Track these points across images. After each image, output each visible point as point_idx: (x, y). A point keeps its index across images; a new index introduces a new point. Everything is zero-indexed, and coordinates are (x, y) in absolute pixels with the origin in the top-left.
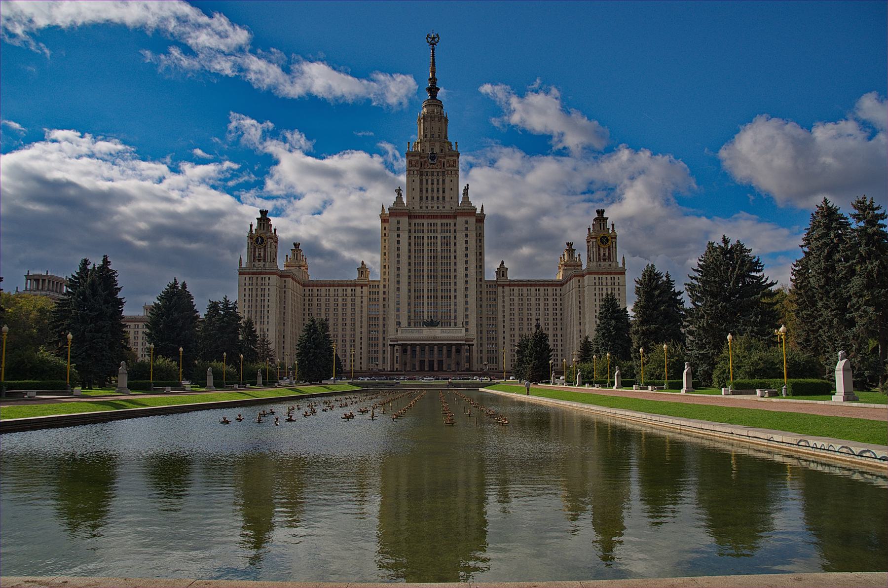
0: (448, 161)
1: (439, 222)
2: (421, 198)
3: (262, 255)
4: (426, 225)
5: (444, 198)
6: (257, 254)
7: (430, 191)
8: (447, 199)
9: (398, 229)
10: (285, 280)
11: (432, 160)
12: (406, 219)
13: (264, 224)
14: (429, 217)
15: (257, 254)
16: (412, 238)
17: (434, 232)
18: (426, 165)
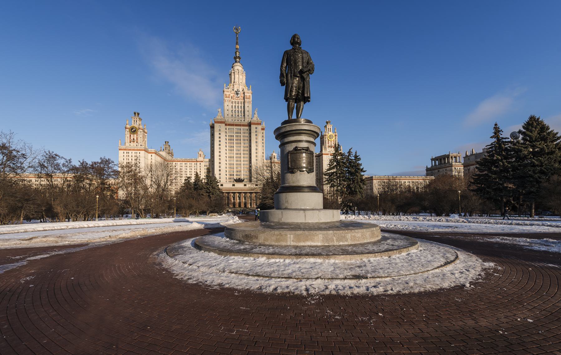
0: (246, 96)
1: (242, 128)
2: (232, 115)
3: (135, 139)
4: (235, 129)
5: (244, 116)
6: (132, 138)
7: (237, 112)
8: (246, 116)
9: (220, 130)
10: (152, 155)
11: (237, 95)
12: (224, 125)
13: (136, 121)
14: (236, 125)
15: (132, 138)
16: (227, 136)
17: (239, 133)
18: (234, 97)
